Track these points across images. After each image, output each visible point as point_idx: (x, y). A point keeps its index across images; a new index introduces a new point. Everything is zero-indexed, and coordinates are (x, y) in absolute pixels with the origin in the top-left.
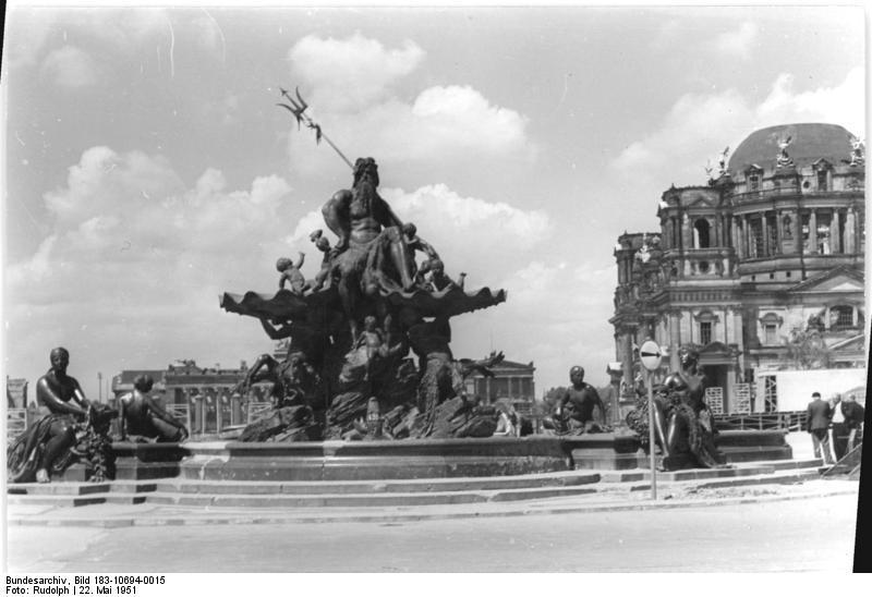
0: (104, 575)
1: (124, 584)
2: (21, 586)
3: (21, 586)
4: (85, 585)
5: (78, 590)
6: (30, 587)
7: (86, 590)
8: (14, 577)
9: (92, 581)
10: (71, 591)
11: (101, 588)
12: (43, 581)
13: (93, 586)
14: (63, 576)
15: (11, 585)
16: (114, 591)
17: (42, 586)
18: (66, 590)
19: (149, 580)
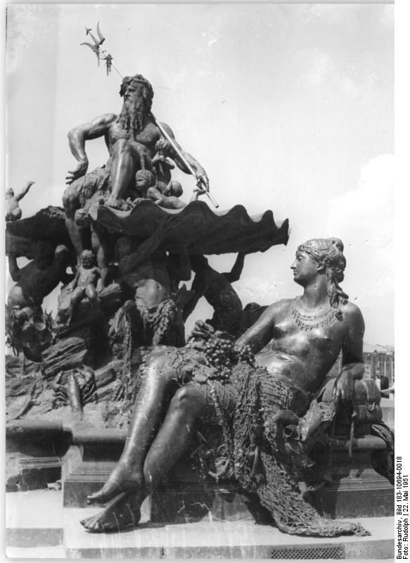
1: (403, 482)
2: (403, 550)
3: (403, 550)
4: (402, 508)
5: (406, 512)
7: (405, 508)
8: (396, 554)
9: (399, 503)
10: (406, 517)
17: (403, 536)
19: (399, 467)
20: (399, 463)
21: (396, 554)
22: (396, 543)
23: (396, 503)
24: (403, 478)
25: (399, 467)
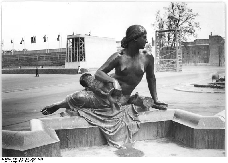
1: (32, 160)
2: (6, 160)
3: (6, 160)
4: (22, 160)
5: (20, 161)
6: (8, 160)
7: (22, 161)
9: (24, 159)
10: (19, 161)
11: (26, 161)
13: (24, 160)
15: (3, 160)
16: (30, 161)
17: (11, 160)
18: (17, 161)
19: (39, 159)
21: (4, 157)
23: (24, 157)
24: (35, 160)
25: (39, 159)
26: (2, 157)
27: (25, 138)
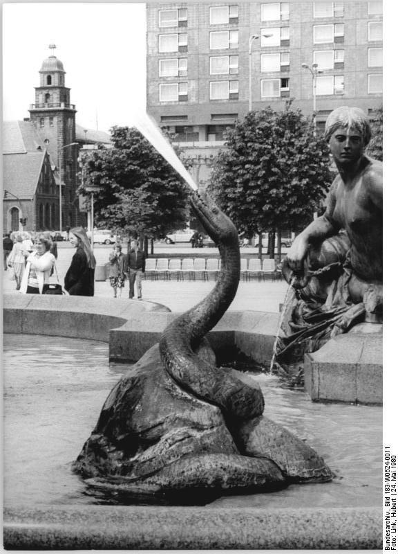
0: (384, 488)
2: (391, 541)
3: (391, 541)
9: (387, 495)
12: (388, 527)
14: (385, 514)
15: (390, 547)
20: (387, 453)
21: (385, 545)
22: (384, 534)
23: (385, 495)
26: (384, 548)
27: (380, 286)
